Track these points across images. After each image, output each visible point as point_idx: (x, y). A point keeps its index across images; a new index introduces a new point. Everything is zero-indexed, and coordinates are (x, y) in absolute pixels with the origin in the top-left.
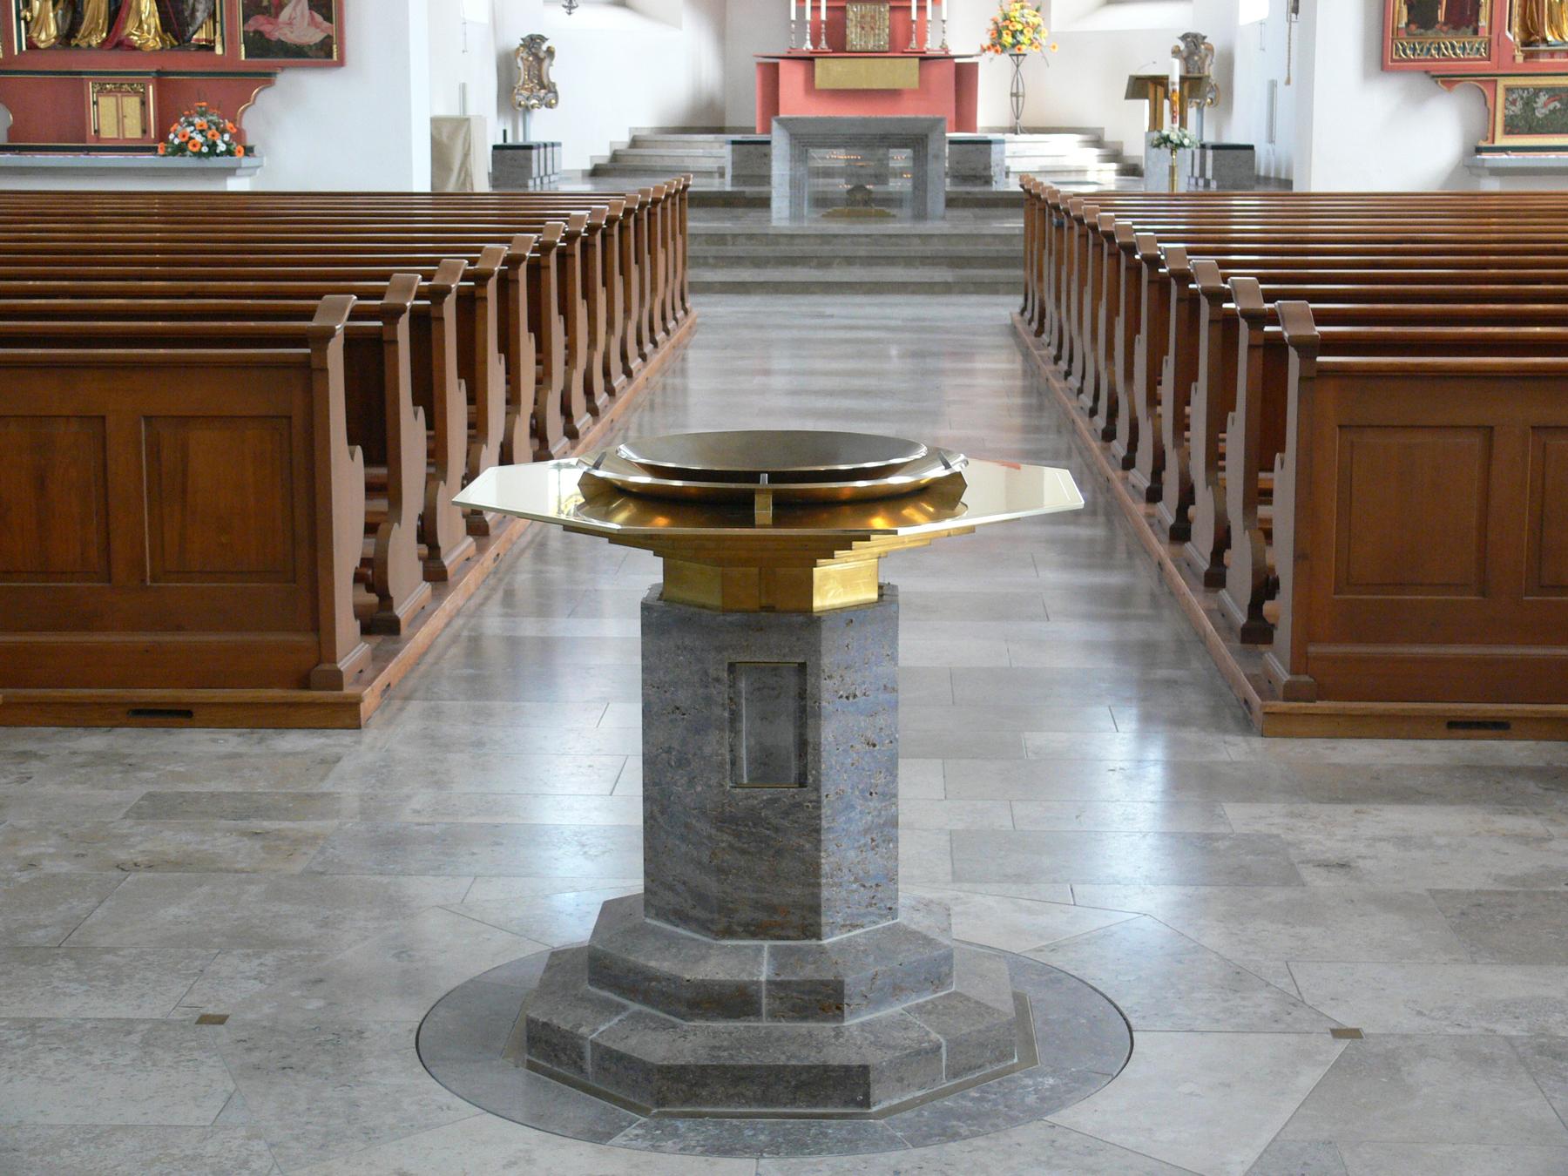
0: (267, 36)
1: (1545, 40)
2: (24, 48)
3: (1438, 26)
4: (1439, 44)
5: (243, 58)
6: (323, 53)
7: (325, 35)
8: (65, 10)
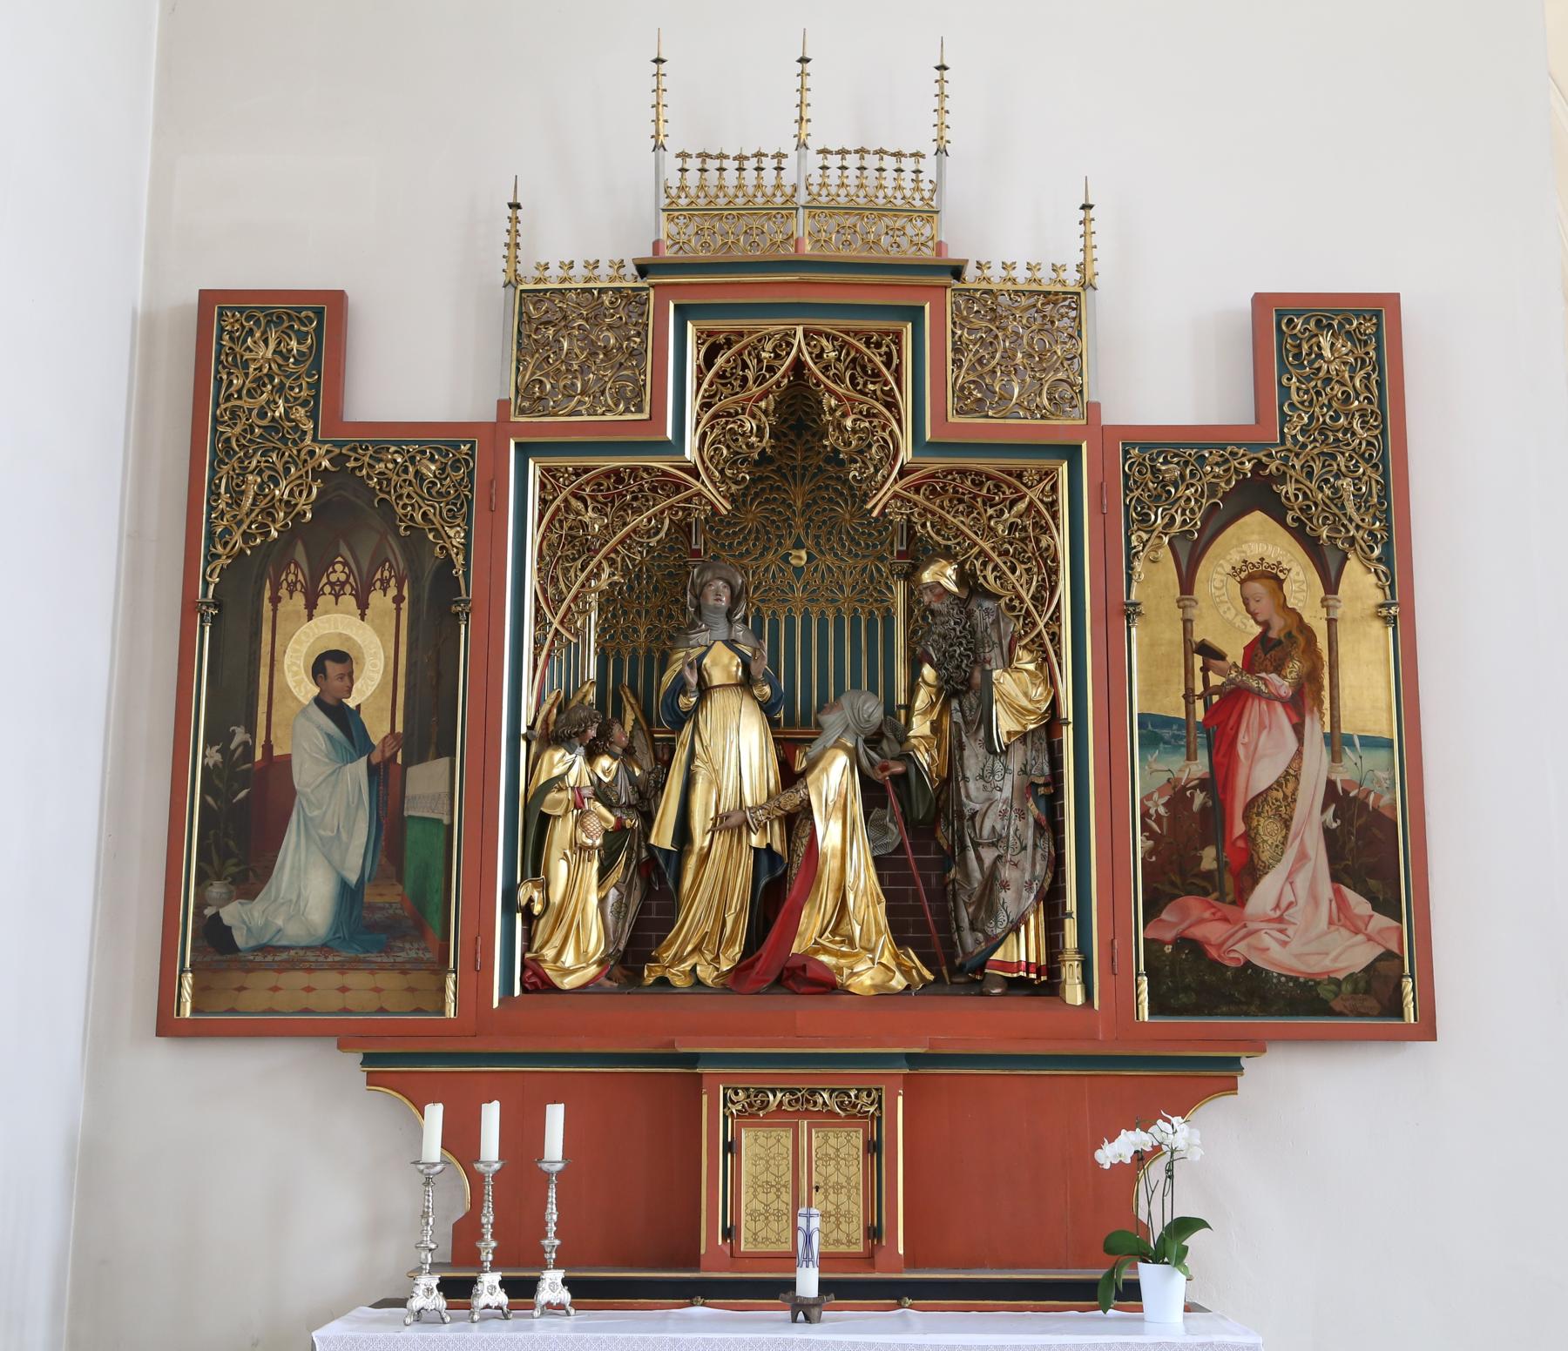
0: (1214, 953)
2: (517, 991)
5: (1145, 1014)
6: (1371, 1003)
7: (1379, 951)
8: (626, 887)
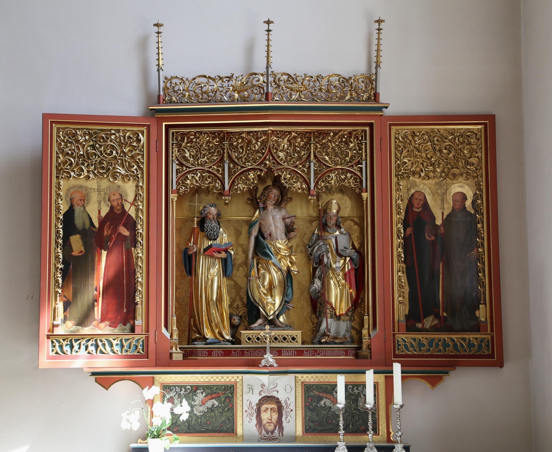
1: (204, 339)
3: (94, 323)
4: (96, 340)
